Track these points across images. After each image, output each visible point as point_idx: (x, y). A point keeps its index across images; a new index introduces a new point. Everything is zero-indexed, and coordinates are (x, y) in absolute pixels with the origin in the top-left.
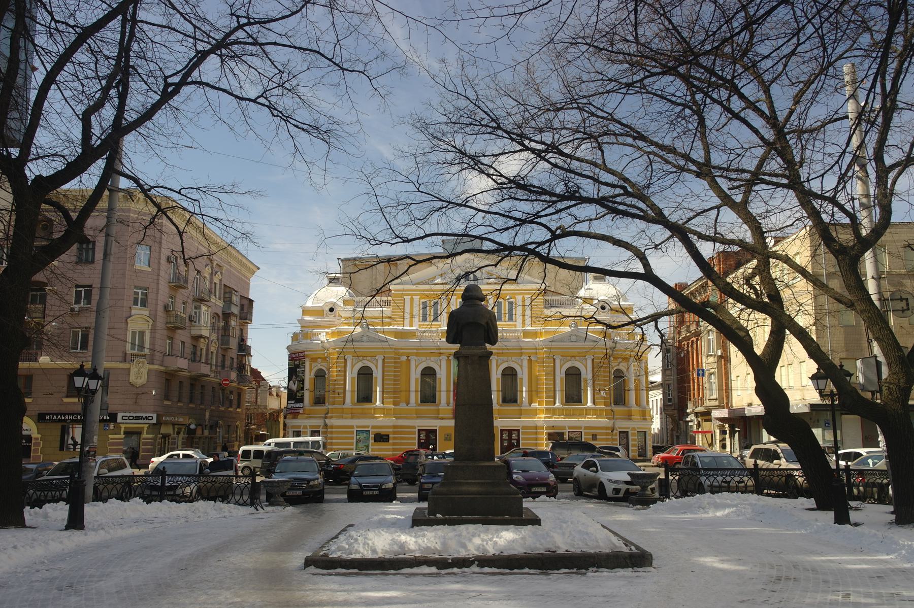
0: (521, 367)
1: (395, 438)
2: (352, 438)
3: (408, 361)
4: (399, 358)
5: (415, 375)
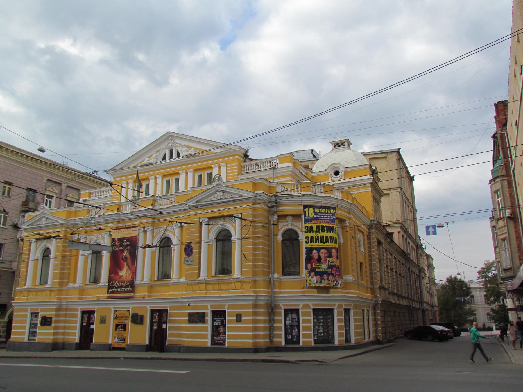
1: (57, 322)
2: (25, 322)
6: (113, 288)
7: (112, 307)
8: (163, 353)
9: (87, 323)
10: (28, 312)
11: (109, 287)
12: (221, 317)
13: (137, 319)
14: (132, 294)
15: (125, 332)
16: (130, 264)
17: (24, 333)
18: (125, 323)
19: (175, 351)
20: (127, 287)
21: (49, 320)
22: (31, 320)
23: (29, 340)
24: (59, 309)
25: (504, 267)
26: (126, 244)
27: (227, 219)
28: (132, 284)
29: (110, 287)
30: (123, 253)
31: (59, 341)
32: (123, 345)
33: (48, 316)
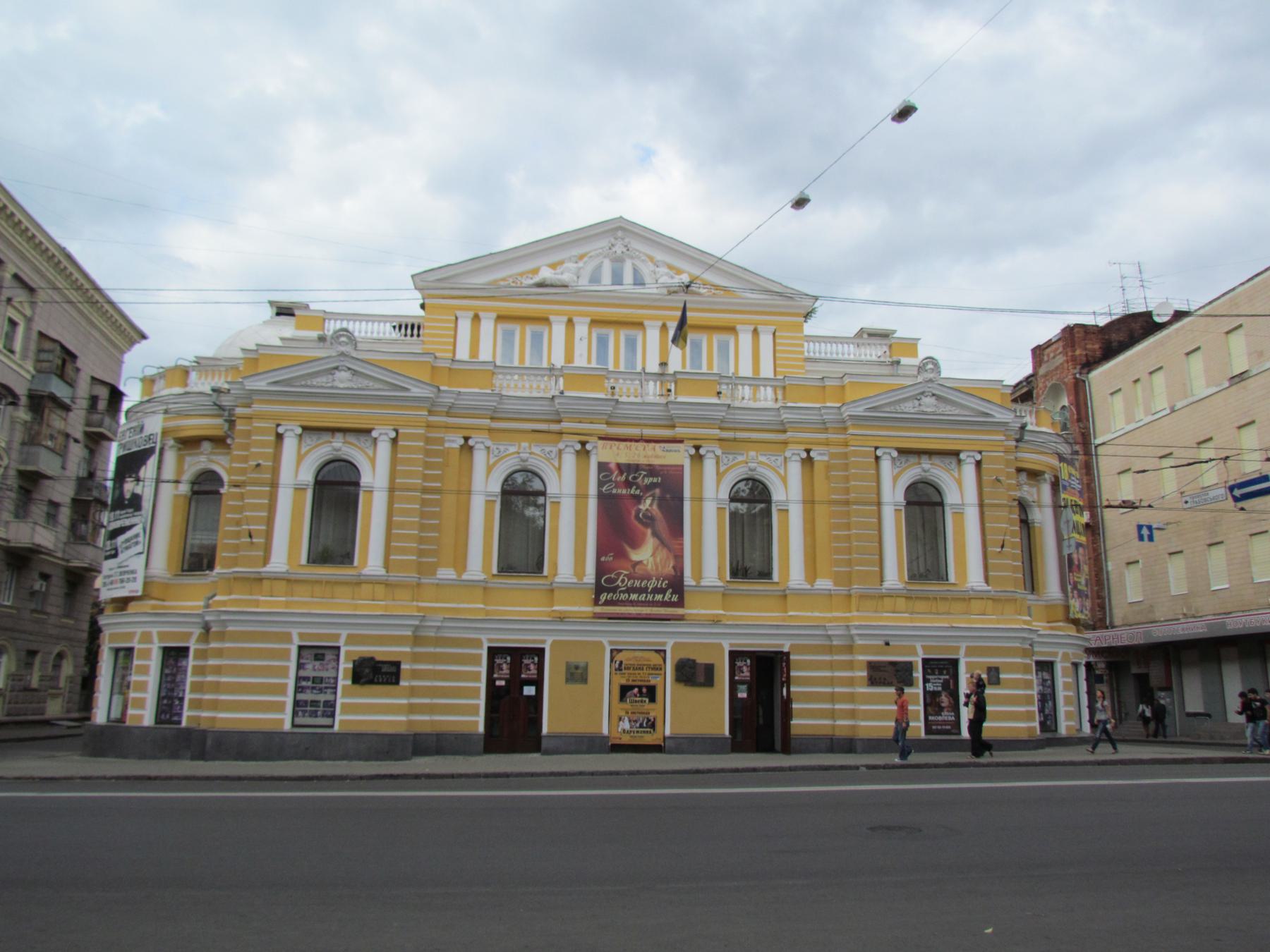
0: (784, 480)
1: (416, 675)
2: (283, 672)
3: (467, 449)
4: (441, 441)
5: (486, 483)
6: (614, 590)
7: (605, 641)
8: (793, 756)
9: (507, 681)
10: (151, 642)
11: (599, 589)
12: (941, 674)
13: (692, 674)
14: (679, 611)
15: (652, 706)
16: (665, 533)
17: (280, 707)
18: (653, 682)
19: (821, 751)
20: (656, 591)
21: (385, 669)
22: (300, 666)
23: (294, 725)
24: (417, 640)
25: (1130, 600)
26: (648, 481)
27: (936, 460)
28: (677, 584)
29: (604, 588)
30: (639, 503)
31: (838, 733)
32: (649, 739)
33: (379, 658)
